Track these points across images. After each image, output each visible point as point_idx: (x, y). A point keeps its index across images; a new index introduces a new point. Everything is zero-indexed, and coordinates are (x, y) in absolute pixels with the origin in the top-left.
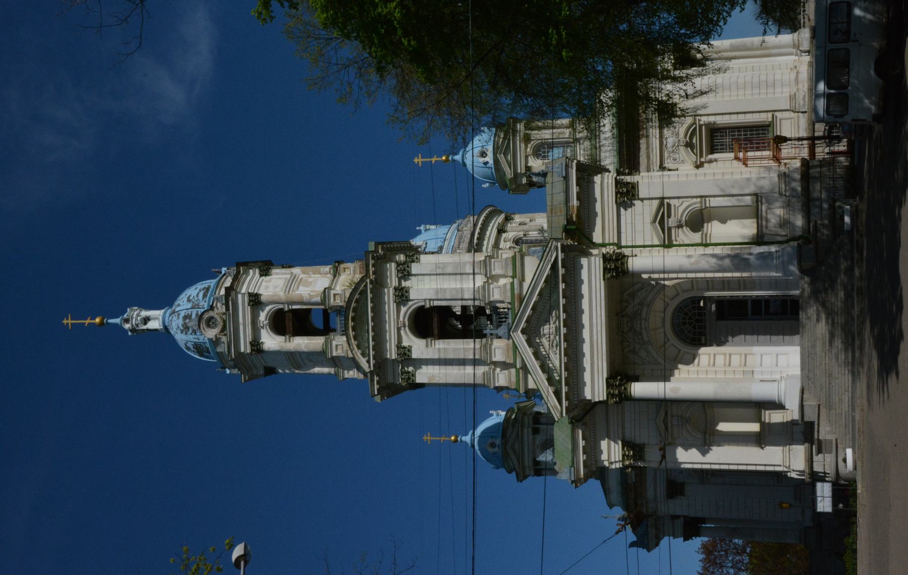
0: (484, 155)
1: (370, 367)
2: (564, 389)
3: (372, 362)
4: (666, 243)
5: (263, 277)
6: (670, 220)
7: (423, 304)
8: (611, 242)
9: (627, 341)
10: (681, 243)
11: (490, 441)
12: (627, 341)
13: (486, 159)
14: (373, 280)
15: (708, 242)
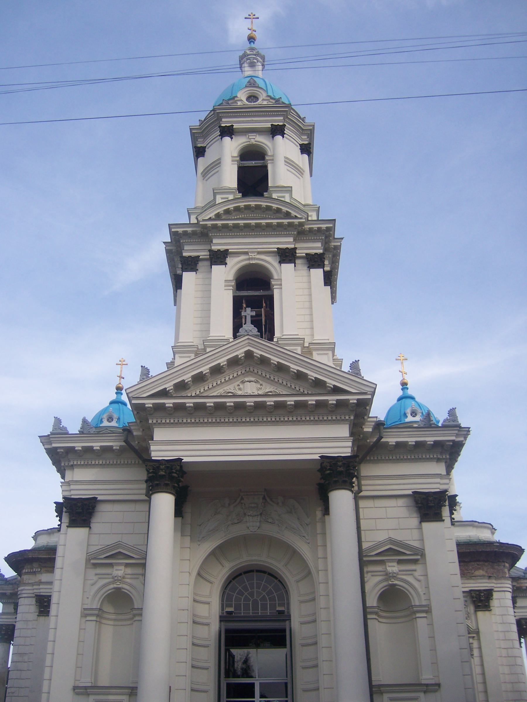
0: (414, 414)
1: (204, 220)
2: (169, 402)
3: (209, 223)
4: (365, 559)
5: (299, 147)
6: (395, 564)
7: (276, 276)
8: (363, 488)
9: (229, 505)
10: (366, 579)
11: (115, 416)
12: (229, 505)
13: (409, 415)
14: (303, 228)
15: (369, 616)
